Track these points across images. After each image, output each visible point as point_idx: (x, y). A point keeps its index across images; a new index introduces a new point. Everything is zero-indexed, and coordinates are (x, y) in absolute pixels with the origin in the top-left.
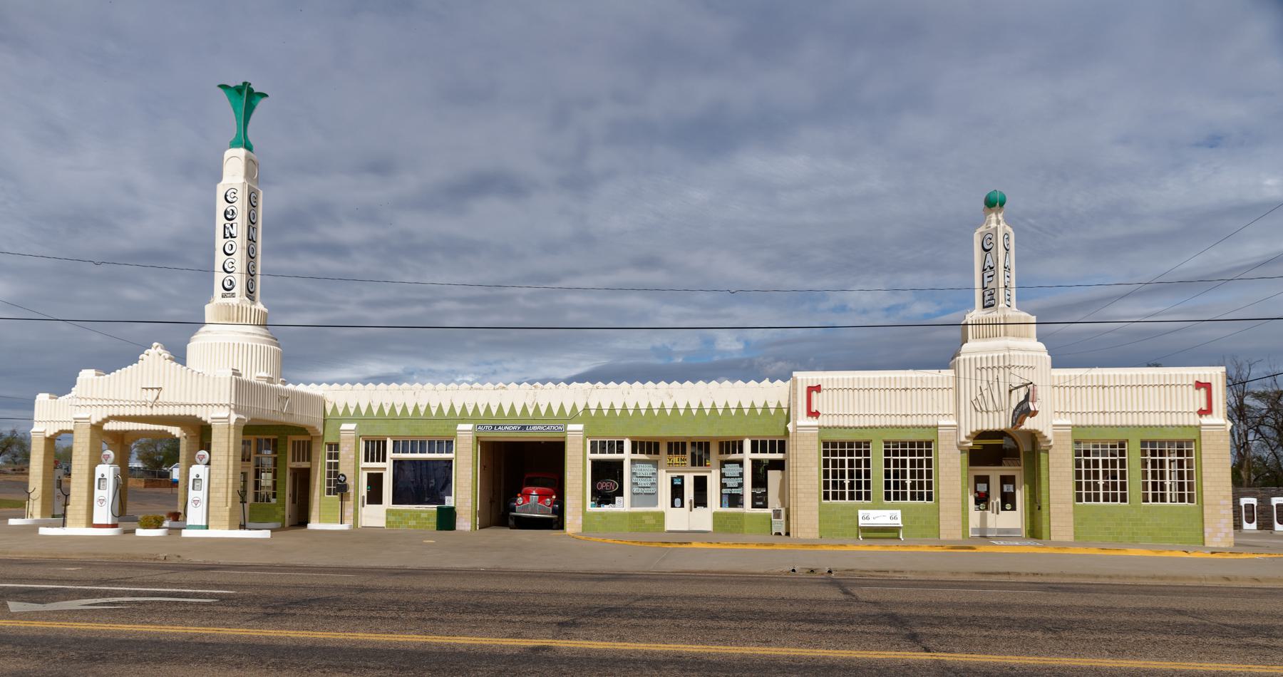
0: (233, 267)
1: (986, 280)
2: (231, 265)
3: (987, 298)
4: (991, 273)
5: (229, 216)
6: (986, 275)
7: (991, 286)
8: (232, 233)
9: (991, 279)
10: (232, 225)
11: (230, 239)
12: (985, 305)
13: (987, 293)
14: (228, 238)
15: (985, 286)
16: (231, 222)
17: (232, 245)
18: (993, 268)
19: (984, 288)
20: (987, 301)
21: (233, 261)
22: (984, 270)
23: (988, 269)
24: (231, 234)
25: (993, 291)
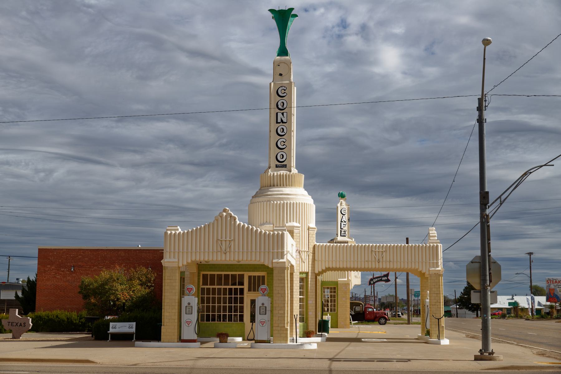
0: (284, 145)
1: (342, 226)
2: (283, 143)
3: (342, 233)
4: (345, 224)
5: (280, 107)
6: (342, 224)
7: (344, 229)
8: (283, 119)
9: (345, 226)
10: (283, 114)
11: (281, 124)
12: (342, 235)
13: (343, 231)
14: (280, 123)
15: (342, 228)
16: (282, 111)
17: (283, 129)
18: (346, 222)
19: (341, 228)
20: (342, 234)
21: (285, 141)
22: (341, 221)
23: (344, 222)
24: (282, 120)
25: (345, 231)
